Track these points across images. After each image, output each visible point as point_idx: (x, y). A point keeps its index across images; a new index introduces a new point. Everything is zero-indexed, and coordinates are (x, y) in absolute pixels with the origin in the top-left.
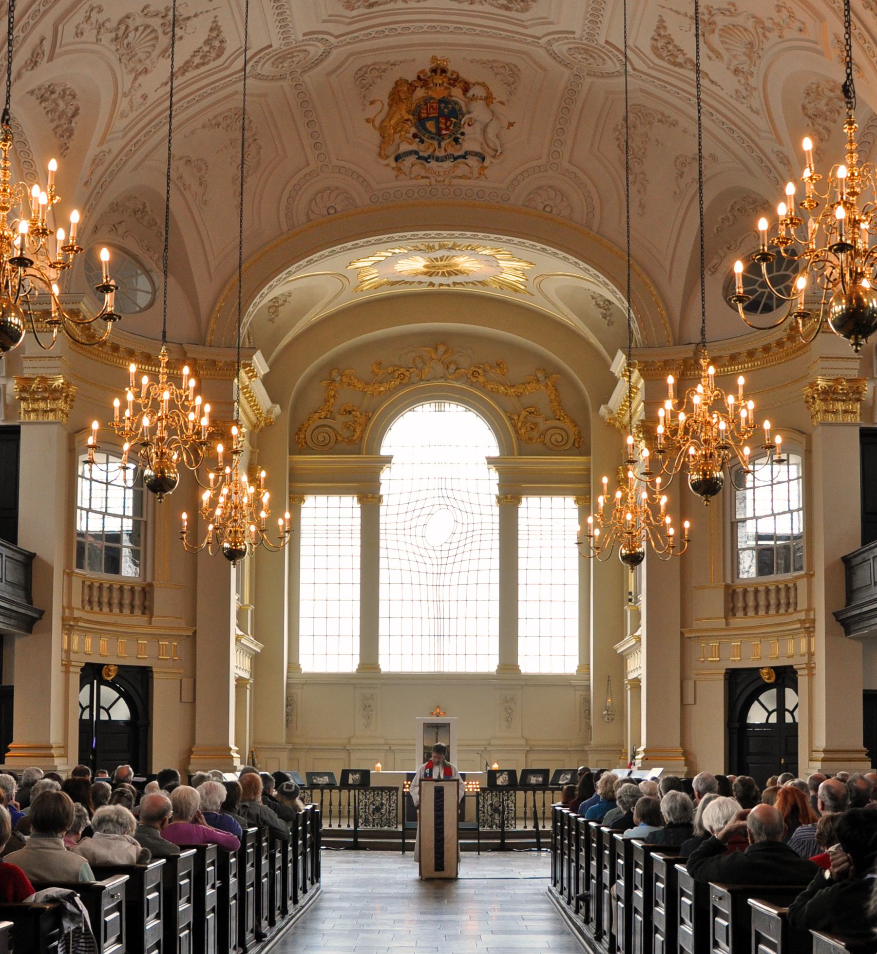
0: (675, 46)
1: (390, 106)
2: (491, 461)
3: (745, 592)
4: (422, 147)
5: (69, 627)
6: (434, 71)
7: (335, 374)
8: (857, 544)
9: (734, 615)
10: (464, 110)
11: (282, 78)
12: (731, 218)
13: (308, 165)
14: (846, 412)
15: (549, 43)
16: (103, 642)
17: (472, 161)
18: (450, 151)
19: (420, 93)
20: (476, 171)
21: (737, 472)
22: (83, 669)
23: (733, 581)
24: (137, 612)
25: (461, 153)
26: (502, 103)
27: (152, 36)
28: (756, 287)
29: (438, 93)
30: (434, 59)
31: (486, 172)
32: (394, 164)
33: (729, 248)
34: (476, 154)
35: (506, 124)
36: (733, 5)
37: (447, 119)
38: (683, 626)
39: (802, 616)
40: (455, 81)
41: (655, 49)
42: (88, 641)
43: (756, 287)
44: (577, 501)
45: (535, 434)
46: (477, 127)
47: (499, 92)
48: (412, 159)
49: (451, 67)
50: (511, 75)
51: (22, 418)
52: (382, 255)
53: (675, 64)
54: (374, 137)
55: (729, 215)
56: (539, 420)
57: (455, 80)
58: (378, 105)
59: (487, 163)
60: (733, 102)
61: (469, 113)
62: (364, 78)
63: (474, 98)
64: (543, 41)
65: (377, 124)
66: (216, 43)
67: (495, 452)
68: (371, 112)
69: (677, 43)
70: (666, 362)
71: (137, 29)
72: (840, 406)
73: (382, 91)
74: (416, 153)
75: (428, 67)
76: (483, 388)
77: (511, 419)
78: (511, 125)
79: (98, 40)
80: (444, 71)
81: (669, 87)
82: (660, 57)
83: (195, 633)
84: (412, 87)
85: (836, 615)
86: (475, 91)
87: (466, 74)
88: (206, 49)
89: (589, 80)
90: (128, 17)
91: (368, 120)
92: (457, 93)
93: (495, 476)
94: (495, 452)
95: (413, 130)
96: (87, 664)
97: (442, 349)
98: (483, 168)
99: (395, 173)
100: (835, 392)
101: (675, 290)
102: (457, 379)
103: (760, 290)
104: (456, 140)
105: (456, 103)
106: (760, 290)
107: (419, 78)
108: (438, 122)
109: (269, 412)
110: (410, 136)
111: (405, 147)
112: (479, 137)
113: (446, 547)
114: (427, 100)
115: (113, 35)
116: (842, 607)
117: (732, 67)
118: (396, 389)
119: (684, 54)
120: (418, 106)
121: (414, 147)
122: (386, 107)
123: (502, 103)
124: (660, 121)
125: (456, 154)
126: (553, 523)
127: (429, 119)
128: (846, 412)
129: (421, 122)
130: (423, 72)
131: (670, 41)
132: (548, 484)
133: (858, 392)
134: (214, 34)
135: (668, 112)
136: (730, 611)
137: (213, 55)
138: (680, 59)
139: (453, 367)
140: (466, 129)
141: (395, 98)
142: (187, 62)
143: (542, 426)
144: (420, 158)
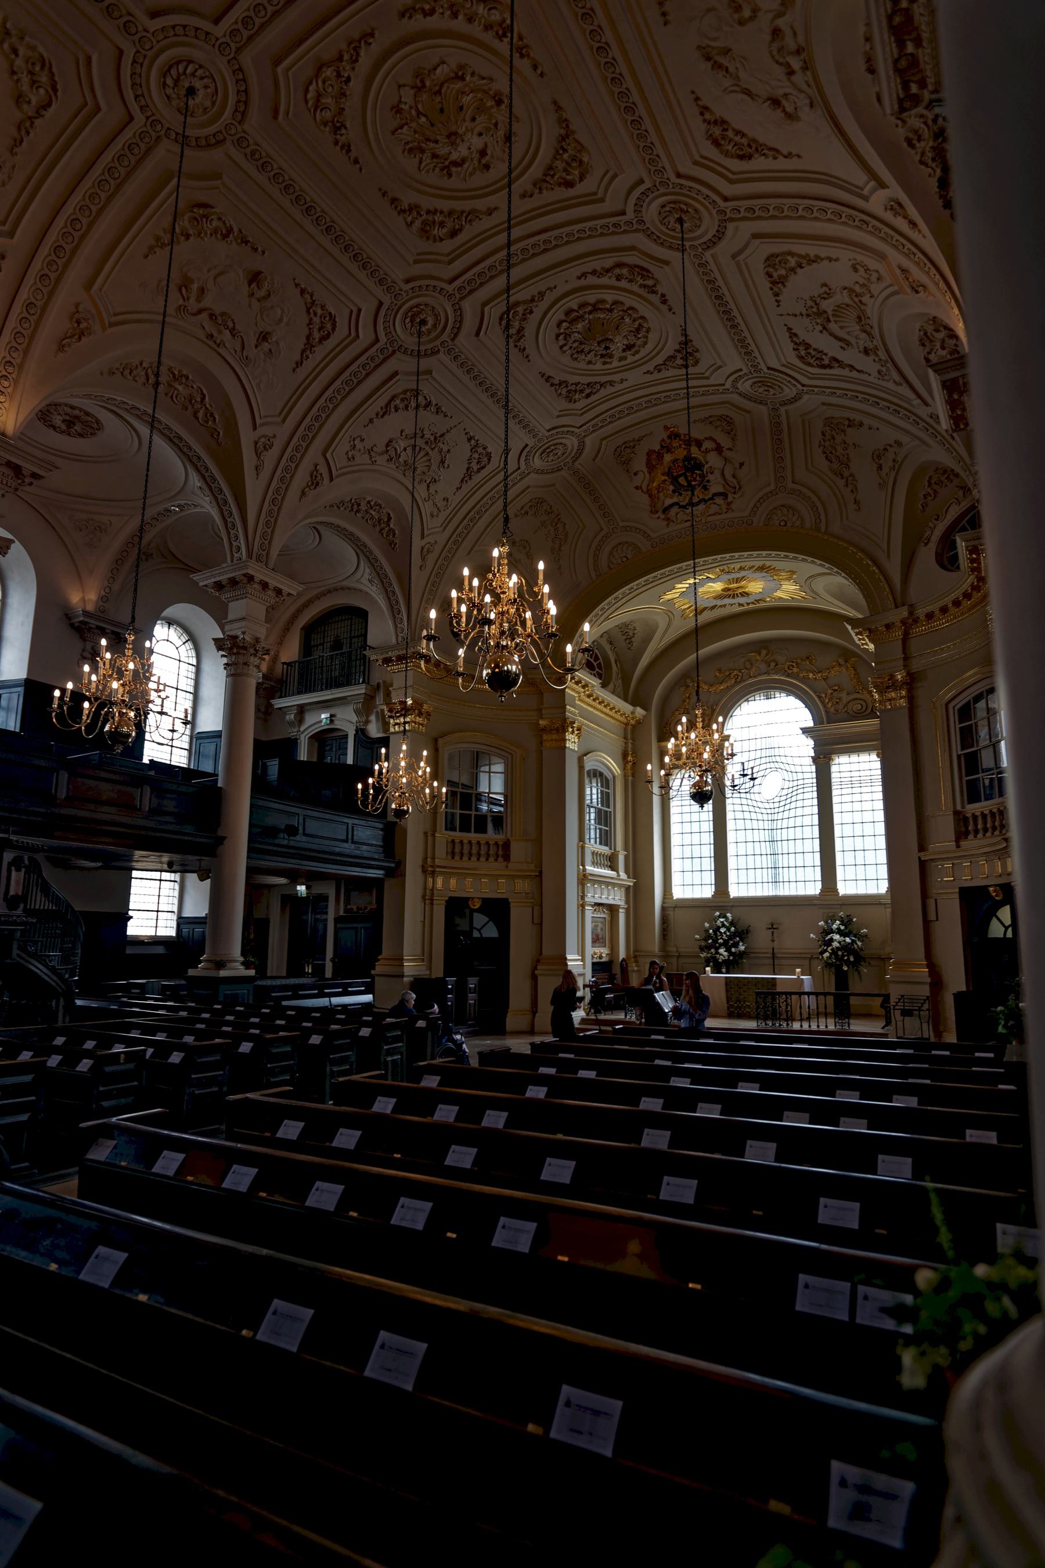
0: (814, 350)
1: (650, 473)
2: (805, 731)
4: (681, 498)
5: (428, 870)
6: (669, 437)
7: (688, 681)
9: (966, 838)
11: (559, 470)
12: (931, 492)
13: (602, 529)
15: (734, 387)
16: (453, 882)
18: (701, 497)
19: (668, 458)
20: (724, 507)
21: (960, 710)
22: (447, 901)
23: (963, 807)
24: (500, 859)
25: (710, 496)
26: (730, 449)
27: (422, 453)
29: (681, 453)
30: (666, 428)
31: (733, 506)
32: (663, 516)
33: (937, 520)
35: (737, 466)
36: (825, 285)
37: (693, 473)
38: (922, 848)
40: (688, 442)
41: (801, 358)
42: (453, 882)
44: (878, 756)
45: (840, 707)
47: (725, 442)
48: (675, 509)
50: (727, 423)
51: (392, 730)
52: (682, 586)
53: (823, 367)
54: (646, 499)
55: (929, 490)
56: (843, 695)
57: (689, 440)
58: (641, 474)
59: (730, 499)
60: (881, 383)
61: (707, 463)
62: (623, 455)
63: (707, 451)
64: (728, 385)
65: (644, 488)
66: (480, 450)
67: (811, 724)
68: (638, 481)
69: (814, 346)
71: (405, 449)
73: (639, 463)
74: (677, 504)
75: (664, 435)
76: (795, 676)
77: (820, 697)
78: (742, 465)
79: (374, 463)
81: (838, 392)
82: (809, 364)
83: (541, 872)
84: (660, 457)
86: (707, 445)
88: (476, 456)
89: (783, 409)
90: (390, 441)
91: (637, 488)
92: (694, 451)
93: (811, 743)
94: (811, 724)
95: (671, 488)
96: (450, 898)
97: (764, 652)
98: (729, 504)
99: (666, 523)
102: (776, 673)
104: (705, 488)
105: (696, 459)
107: (662, 446)
108: (686, 478)
109: (633, 713)
110: (670, 492)
111: (668, 502)
112: (720, 480)
113: (777, 799)
114: (675, 461)
115: (386, 457)
117: (862, 349)
118: (733, 686)
119: (826, 355)
120: (670, 468)
121: (675, 500)
122: (647, 475)
123: (730, 449)
124: (849, 426)
125: (706, 498)
126: (860, 774)
127: (681, 475)
129: (675, 480)
130: (663, 440)
131: (808, 346)
132: (853, 745)
134: (473, 442)
135: (852, 416)
137: (486, 459)
138: (826, 362)
139: (773, 664)
140: (710, 477)
141: (651, 467)
142: (468, 469)
143: (845, 698)
144: (681, 507)
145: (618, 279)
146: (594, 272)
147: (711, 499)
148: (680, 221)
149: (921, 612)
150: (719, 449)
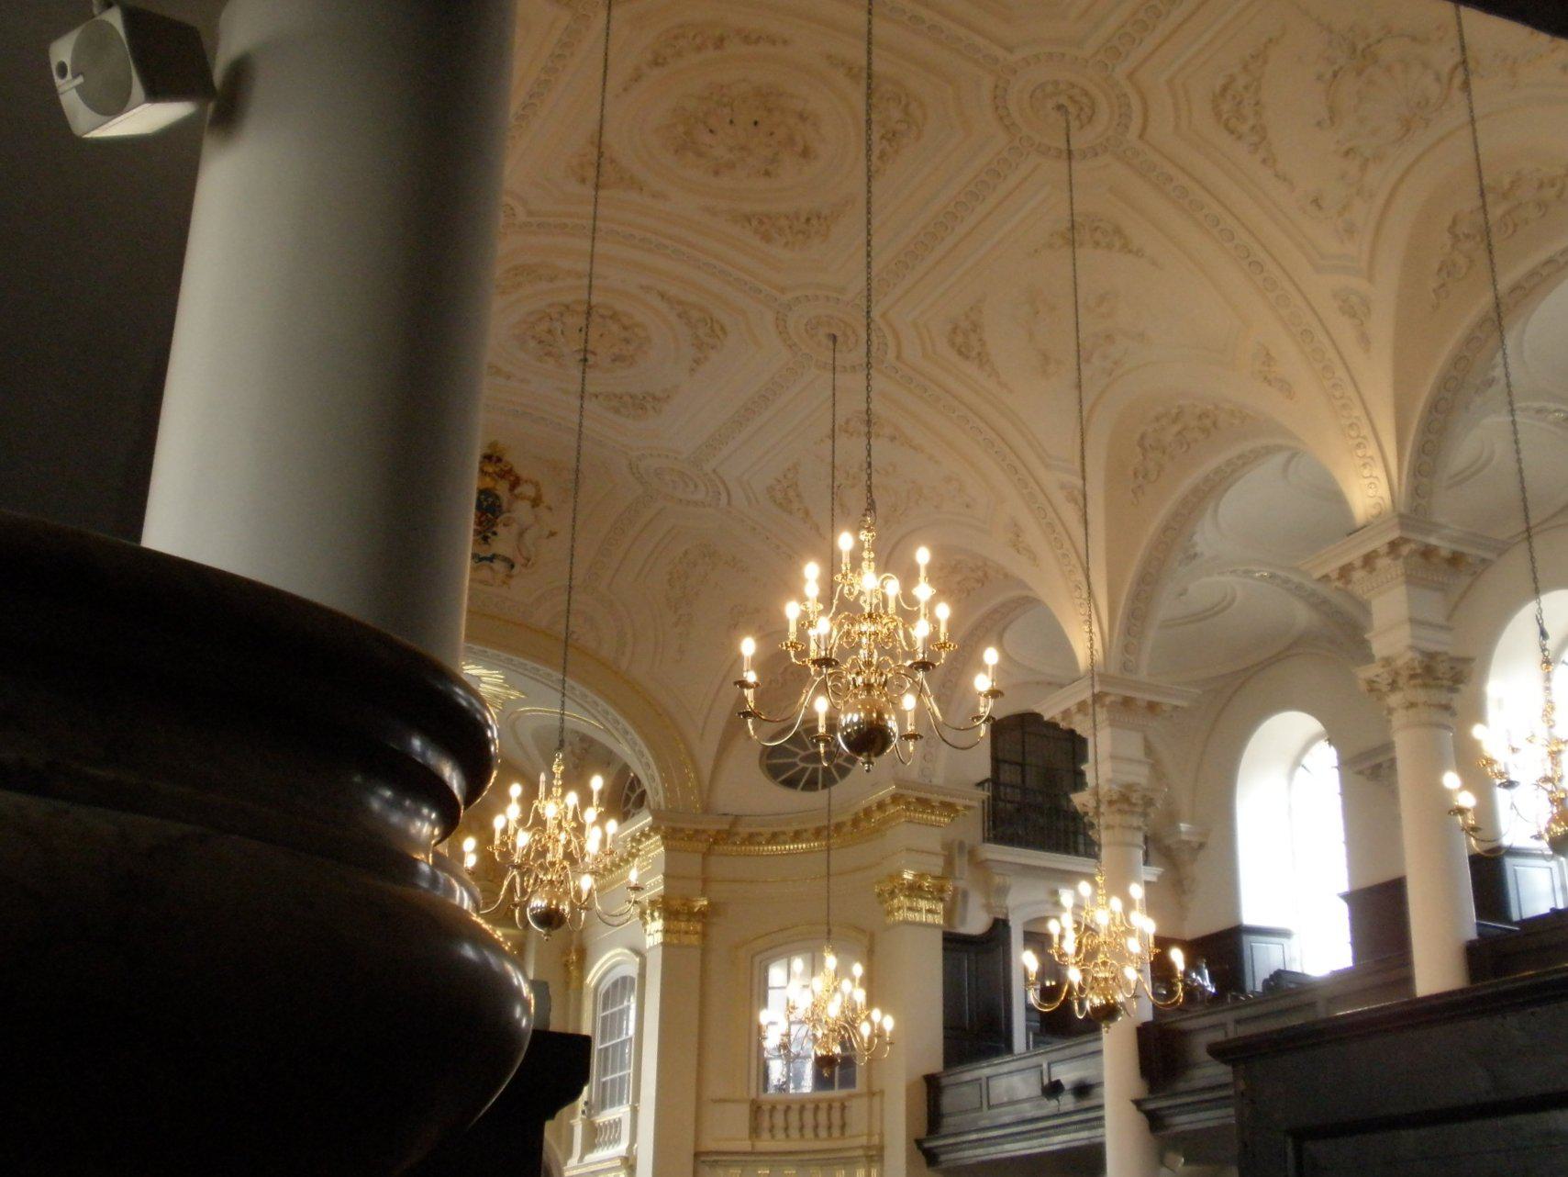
3: (773, 1108)
8: (935, 1064)
10: (505, 505)
14: (929, 911)
17: (498, 565)
26: (550, 509)
28: (797, 760)
34: (506, 559)
39: (863, 1140)
43: (797, 760)
46: (515, 528)
47: (549, 496)
49: (507, 457)
59: (515, 571)
70: (697, 831)
72: (923, 904)
78: (552, 534)
80: (499, 460)
85: (919, 1143)
86: (527, 490)
87: (522, 472)
98: (510, 576)
100: (920, 888)
101: (706, 751)
103: (802, 765)
105: (497, 497)
106: (802, 765)
116: (923, 1135)
123: (550, 509)
128: (929, 911)
133: (941, 890)
136: (755, 1131)
140: (500, 529)
145: (679, 316)
146: (662, 296)
147: (492, 559)
148: (834, 338)
149: (743, 830)
150: (536, 502)
